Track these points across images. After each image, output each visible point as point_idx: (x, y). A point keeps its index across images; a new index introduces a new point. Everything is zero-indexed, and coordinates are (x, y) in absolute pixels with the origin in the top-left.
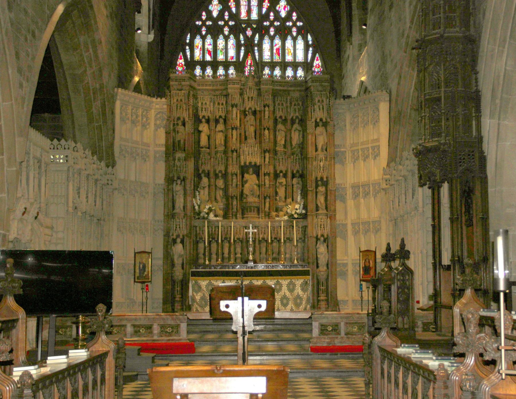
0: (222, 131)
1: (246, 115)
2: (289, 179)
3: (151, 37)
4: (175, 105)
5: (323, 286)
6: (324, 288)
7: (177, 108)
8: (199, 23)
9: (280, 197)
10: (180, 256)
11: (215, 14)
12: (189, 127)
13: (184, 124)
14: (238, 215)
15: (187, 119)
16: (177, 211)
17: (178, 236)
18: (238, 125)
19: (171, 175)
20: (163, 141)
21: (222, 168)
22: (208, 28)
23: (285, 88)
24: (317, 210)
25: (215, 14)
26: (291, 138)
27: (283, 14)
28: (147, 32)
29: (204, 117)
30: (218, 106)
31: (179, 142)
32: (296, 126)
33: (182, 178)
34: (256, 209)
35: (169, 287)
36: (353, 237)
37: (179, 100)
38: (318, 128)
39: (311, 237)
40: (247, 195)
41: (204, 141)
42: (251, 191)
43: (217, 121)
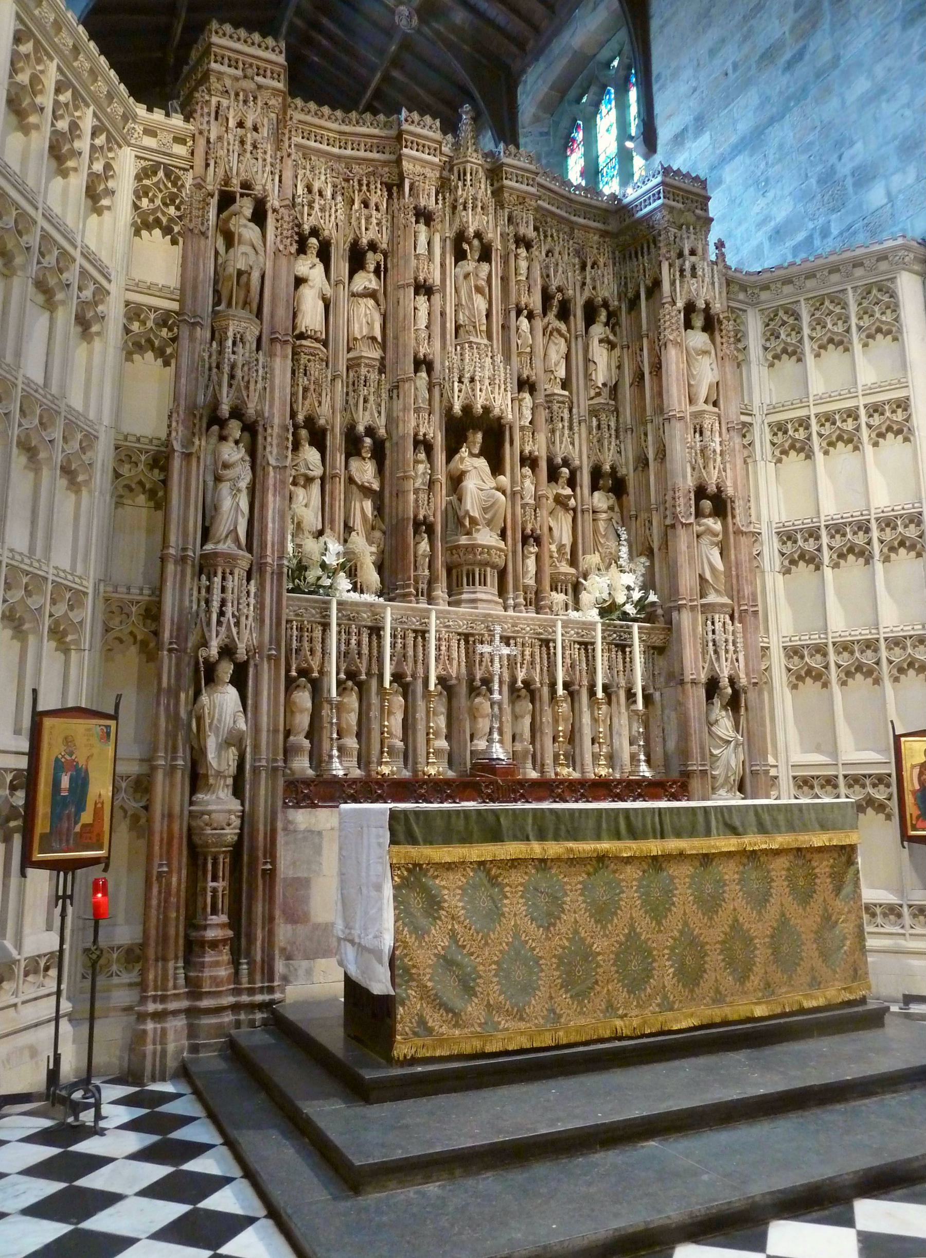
0: (373, 295)
9: (561, 547)
10: (235, 740)
18: (438, 282)
26: (588, 361)
30: (365, 211)
32: (598, 330)
34: (492, 577)
35: (178, 880)
36: (787, 691)
37: (249, 124)
39: (694, 682)
40: (473, 521)
42: (485, 510)
43: (357, 261)
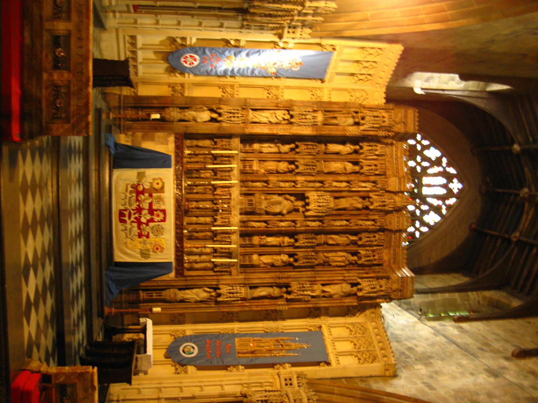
1: (364, 198)
2: (287, 250)
3: (418, 91)
4: (380, 115)
5: (156, 296)
6: (154, 294)
7: (374, 116)
8: (419, 137)
11: (426, 153)
12: (354, 131)
13: (357, 124)
14: (244, 189)
15: (362, 128)
16: (251, 114)
17: (220, 115)
19: (295, 108)
20: (334, 99)
21: (301, 168)
22: (415, 146)
23: (393, 244)
24: (251, 288)
25: (426, 153)
27: (426, 218)
28: (423, 87)
29: (361, 148)
31: (335, 118)
33: (293, 120)
35: (155, 103)
38: (350, 286)
41: (334, 147)
43: (356, 163)
